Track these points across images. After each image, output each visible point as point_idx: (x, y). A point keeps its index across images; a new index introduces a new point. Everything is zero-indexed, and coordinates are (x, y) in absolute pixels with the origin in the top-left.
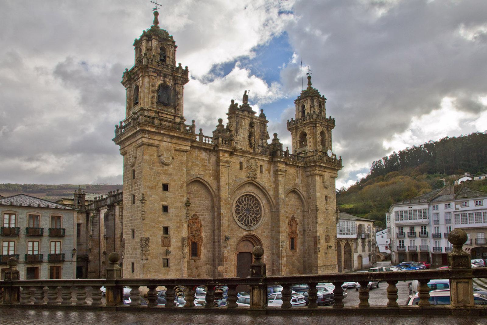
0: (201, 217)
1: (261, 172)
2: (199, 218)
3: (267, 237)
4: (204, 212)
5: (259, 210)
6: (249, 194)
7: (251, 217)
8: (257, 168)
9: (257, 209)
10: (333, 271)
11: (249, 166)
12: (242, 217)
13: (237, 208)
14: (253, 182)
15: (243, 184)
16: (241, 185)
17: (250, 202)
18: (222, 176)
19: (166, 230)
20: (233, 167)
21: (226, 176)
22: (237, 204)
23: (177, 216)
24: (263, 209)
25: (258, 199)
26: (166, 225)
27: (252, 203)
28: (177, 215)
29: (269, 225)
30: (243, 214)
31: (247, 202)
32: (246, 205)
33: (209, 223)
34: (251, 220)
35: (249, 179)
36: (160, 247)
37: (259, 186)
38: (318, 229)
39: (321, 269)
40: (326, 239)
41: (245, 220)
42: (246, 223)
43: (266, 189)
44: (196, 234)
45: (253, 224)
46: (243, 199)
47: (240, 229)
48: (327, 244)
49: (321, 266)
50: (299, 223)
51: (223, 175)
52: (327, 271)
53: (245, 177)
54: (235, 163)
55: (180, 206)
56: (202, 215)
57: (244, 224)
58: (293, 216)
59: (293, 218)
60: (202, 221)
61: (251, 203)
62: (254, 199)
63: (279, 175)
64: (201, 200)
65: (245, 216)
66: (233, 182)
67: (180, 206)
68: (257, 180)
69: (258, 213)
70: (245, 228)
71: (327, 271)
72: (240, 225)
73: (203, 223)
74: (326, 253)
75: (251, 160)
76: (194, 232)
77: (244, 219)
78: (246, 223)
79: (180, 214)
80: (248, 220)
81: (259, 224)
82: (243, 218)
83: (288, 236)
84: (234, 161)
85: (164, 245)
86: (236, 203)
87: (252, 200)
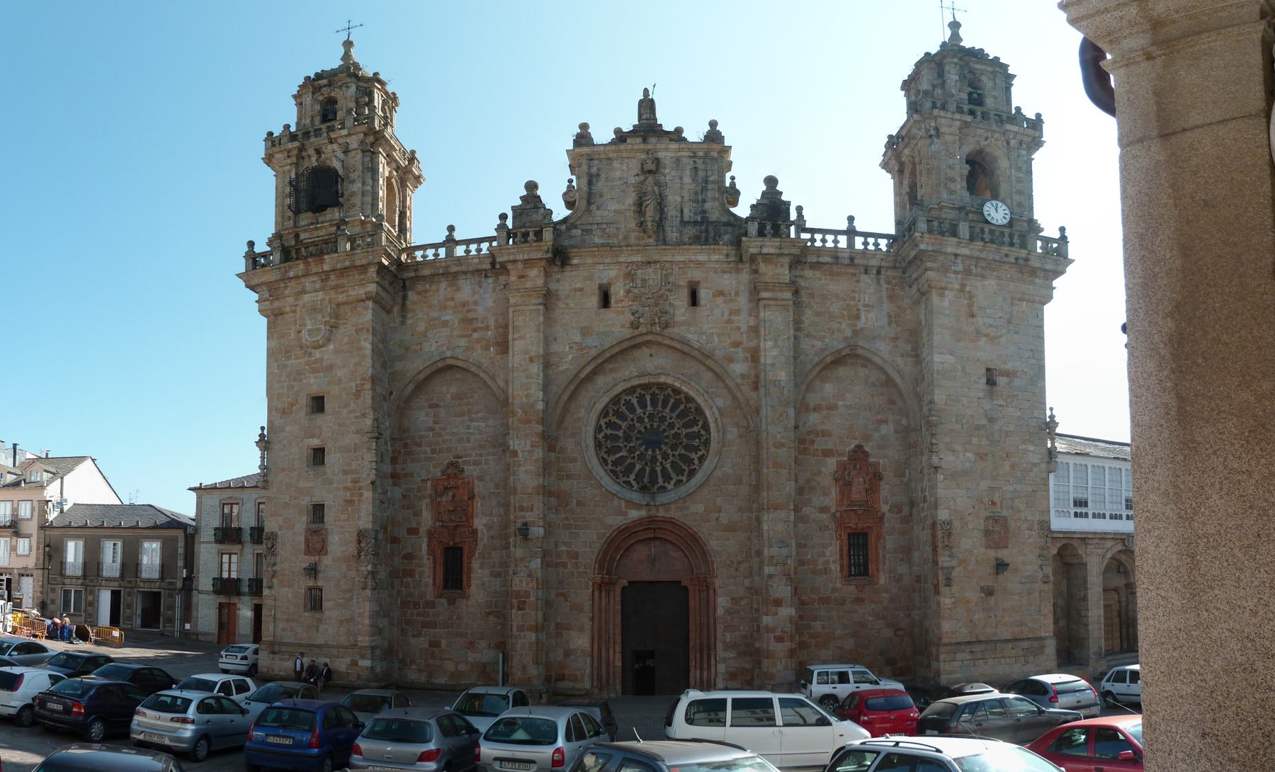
0: (470, 470)
1: (694, 300)
2: (466, 473)
3: (731, 528)
4: (481, 455)
5: (703, 432)
7: (665, 456)
9: (695, 429)
10: (1027, 662)
11: (636, 291)
13: (609, 432)
14: (659, 339)
15: (617, 349)
16: (608, 355)
17: (664, 406)
19: (318, 511)
22: (607, 420)
23: (345, 472)
24: (712, 426)
25: (692, 393)
26: (317, 499)
28: (345, 468)
29: (740, 482)
30: (631, 451)
31: (649, 408)
32: (646, 420)
33: (497, 486)
35: (636, 332)
36: (302, 557)
37: (686, 349)
38: (941, 492)
39: (960, 656)
40: (987, 533)
41: (643, 469)
42: (646, 480)
44: (451, 520)
45: (673, 482)
46: (635, 401)
47: (616, 502)
48: (992, 554)
49: (959, 644)
50: (888, 475)
52: (991, 662)
53: (623, 326)
55: (355, 444)
56: (476, 463)
57: (634, 483)
58: (859, 447)
59: (859, 455)
60: (476, 482)
61: (667, 410)
64: (472, 420)
65: (642, 457)
67: (355, 444)
68: (676, 330)
69: (696, 442)
70: (636, 497)
71: (991, 662)
72: (615, 488)
73: (479, 488)
74: (989, 592)
75: (640, 271)
76: (445, 517)
77: (638, 467)
78: (646, 480)
79: (354, 466)
80: (653, 472)
81: (695, 482)
82: (632, 466)
83: (832, 526)
85: (309, 550)
86: (604, 413)
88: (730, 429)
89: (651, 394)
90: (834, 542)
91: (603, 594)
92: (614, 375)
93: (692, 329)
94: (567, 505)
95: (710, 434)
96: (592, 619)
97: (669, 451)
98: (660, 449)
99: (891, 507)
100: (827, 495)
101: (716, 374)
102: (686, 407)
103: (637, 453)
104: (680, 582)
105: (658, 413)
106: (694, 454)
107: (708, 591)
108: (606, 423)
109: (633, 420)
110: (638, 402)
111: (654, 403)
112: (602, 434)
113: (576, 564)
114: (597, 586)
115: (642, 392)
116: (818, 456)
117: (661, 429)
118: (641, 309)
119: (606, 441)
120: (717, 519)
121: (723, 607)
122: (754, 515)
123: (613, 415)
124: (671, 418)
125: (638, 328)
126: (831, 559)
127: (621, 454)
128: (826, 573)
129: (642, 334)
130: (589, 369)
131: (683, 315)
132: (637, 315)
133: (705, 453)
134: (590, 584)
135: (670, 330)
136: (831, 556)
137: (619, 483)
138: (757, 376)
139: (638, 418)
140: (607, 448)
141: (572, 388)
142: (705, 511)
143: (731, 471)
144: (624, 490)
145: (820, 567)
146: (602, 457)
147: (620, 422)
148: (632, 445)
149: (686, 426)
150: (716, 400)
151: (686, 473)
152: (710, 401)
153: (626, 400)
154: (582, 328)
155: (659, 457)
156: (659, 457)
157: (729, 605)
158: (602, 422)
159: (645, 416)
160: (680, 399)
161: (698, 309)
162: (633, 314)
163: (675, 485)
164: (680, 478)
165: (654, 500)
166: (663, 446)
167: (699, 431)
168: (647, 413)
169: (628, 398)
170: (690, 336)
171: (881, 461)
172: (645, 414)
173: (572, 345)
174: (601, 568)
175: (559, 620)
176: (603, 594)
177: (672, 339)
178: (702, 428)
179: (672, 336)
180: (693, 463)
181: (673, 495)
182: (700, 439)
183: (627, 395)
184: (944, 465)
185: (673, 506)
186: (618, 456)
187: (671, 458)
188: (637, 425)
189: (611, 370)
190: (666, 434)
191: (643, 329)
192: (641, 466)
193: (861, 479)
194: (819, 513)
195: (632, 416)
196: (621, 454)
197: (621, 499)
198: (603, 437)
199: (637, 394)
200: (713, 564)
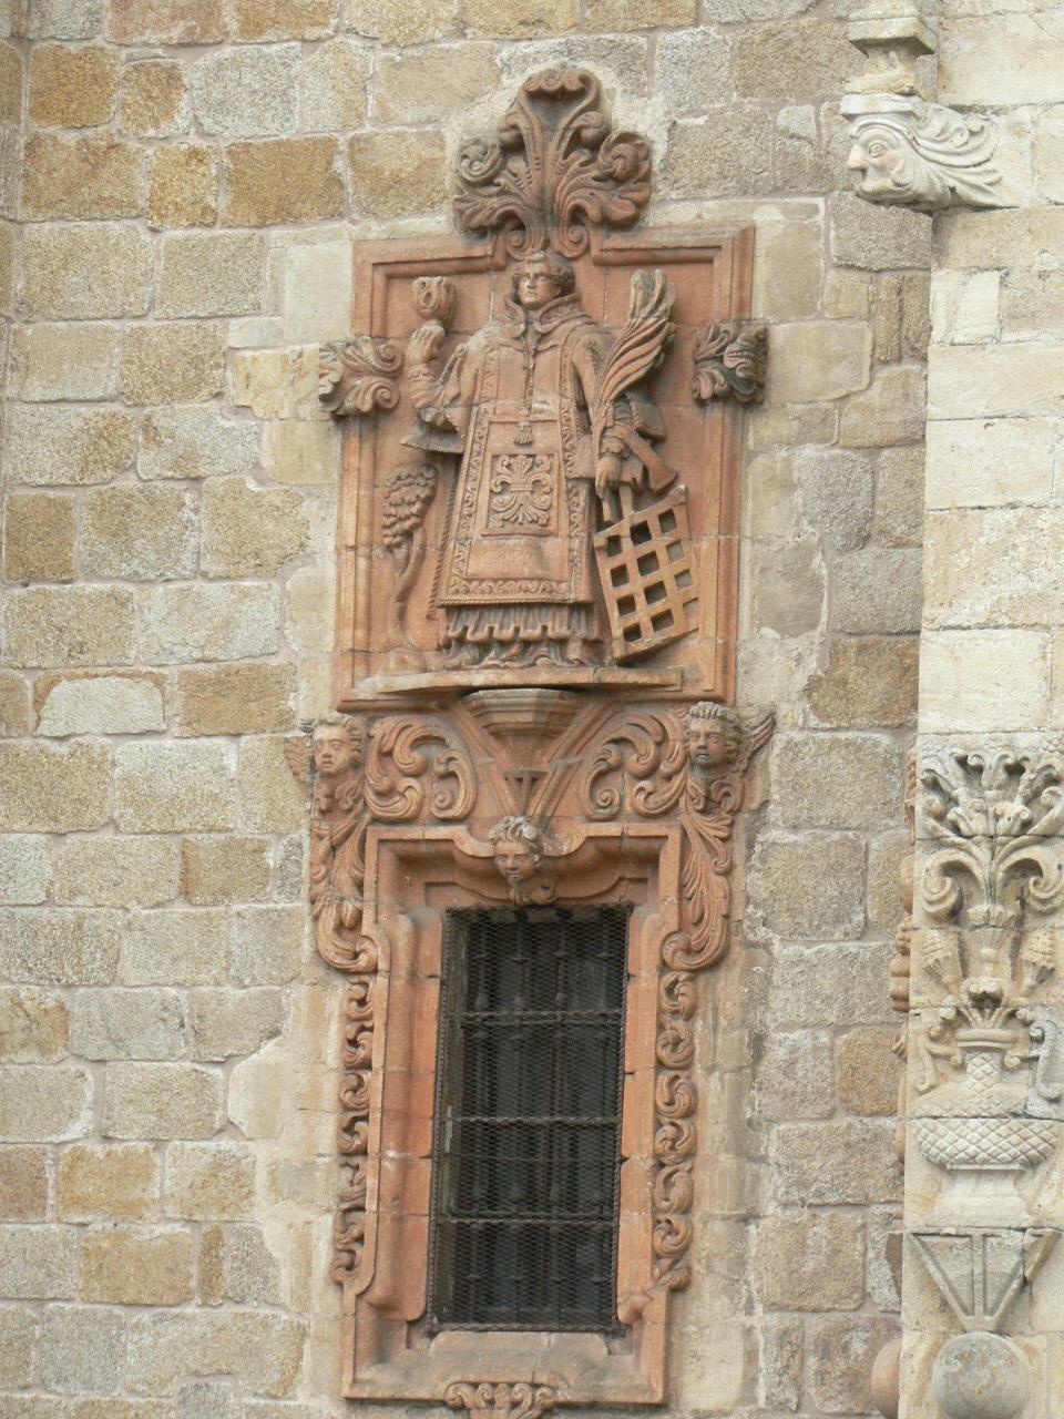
58: (550, 98)
90: (298, 995)
99: (834, 654)
100: (272, 563)
116: (205, 217)
126: (262, 1154)
128: (209, 1289)
136: (269, 1131)
145: (157, 1230)
171: (768, 217)
184: (1013, 183)
193: (552, 402)
194: (197, 725)
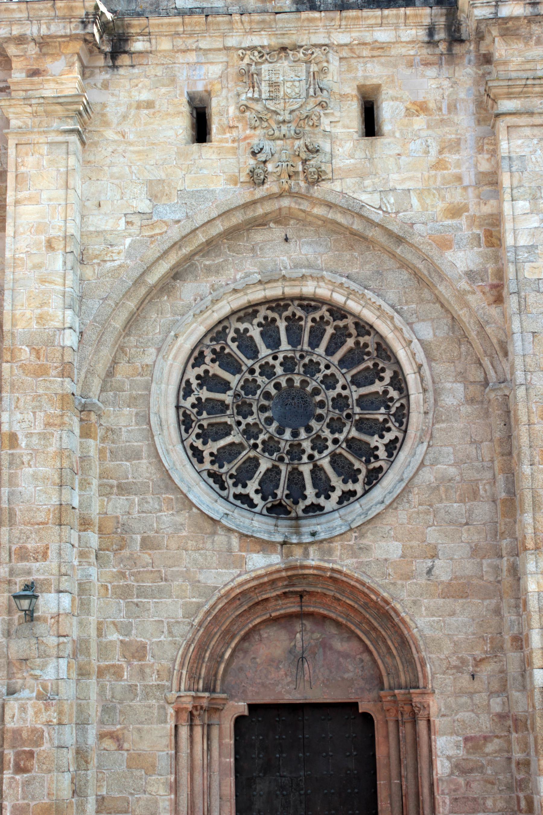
6: (291, 290)
8: (323, 105)
9: (378, 387)
11: (258, 107)
12: (244, 455)
13: (205, 394)
15: (219, 227)
16: (201, 238)
18: (17, 203)
20: (131, 137)
21: (45, 196)
22: (200, 370)
24: (412, 379)
25: (369, 316)
27: (330, 351)
29: (475, 495)
31: (285, 345)
32: (279, 370)
34: (317, 470)
35: (260, 192)
37: (357, 225)
41: (274, 471)
42: (281, 492)
43: (416, 240)
45: (335, 496)
46: (255, 332)
51: (21, 195)
54: (150, 105)
57: (257, 499)
61: (321, 350)
62: (350, 321)
63: (502, 124)
66: (134, 230)
68: (337, 186)
69: (380, 415)
75: (265, 67)
78: (281, 492)
81: (377, 493)
84: (145, 96)
87: (330, 331)
88: (448, 385)
89: (287, 319)
91: (198, 731)
92: (213, 279)
93: (367, 182)
94: (121, 548)
95: (408, 396)
96: (175, 787)
97: (326, 433)
98: (309, 429)
101: (416, 275)
102: (357, 343)
103: (262, 437)
104: (355, 705)
105: (302, 357)
106: (376, 437)
107: (414, 722)
108: (198, 377)
109: (252, 371)
110: (262, 334)
111: (294, 340)
112: (192, 399)
113: (142, 671)
114: (185, 716)
115: (271, 315)
117: (309, 389)
118: (268, 145)
119: (199, 413)
120: (429, 572)
121: (449, 758)
122: (505, 563)
123: (213, 361)
124: (327, 367)
125: (263, 183)
127: (228, 440)
129: (271, 197)
130: (164, 267)
131: (351, 156)
132: (262, 157)
133: (400, 435)
134: (171, 711)
135: (325, 186)
137: (226, 499)
138: (500, 274)
139: (261, 367)
140: (201, 427)
141: (132, 305)
142: (403, 556)
143: (453, 471)
144: (237, 511)
146: (192, 447)
147: (226, 375)
148: (250, 420)
149: (356, 382)
150: (418, 326)
151: (361, 477)
152: (406, 330)
153: (237, 331)
154: (150, 183)
155: (307, 445)
156: (307, 445)
157: (461, 753)
158: (192, 374)
159: (277, 363)
160: (346, 327)
161: (378, 141)
162: (254, 154)
163: (340, 501)
164: (350, 486)
165: (298, 533)
166: (313, 423)
167: (386, 392)
168: (281, 356)
169: (242, 327)
170: (364, 197)
172: (275, 358)
173: (130, 218)
174: (193, 677)
175: (104, 792)
176: (198, 731)
177: (330, 205)
178: (390, 384)
179: (330, 198)
180: (377, 457)
181: (339, 522)
182: (388, 407)
183: (239, 320)
185: (337, 545)
186: (222, 443)
187: (331, 447)
188: (261, 380)
189: (208, 270)
190: (318, 398)
191: (271, 187)
192: (269, 465)
195: (250, 363)
196: (228, 440)
197: (230, 530)
198: (193, 406)
199: (260, 319)
200: (423, 665)
